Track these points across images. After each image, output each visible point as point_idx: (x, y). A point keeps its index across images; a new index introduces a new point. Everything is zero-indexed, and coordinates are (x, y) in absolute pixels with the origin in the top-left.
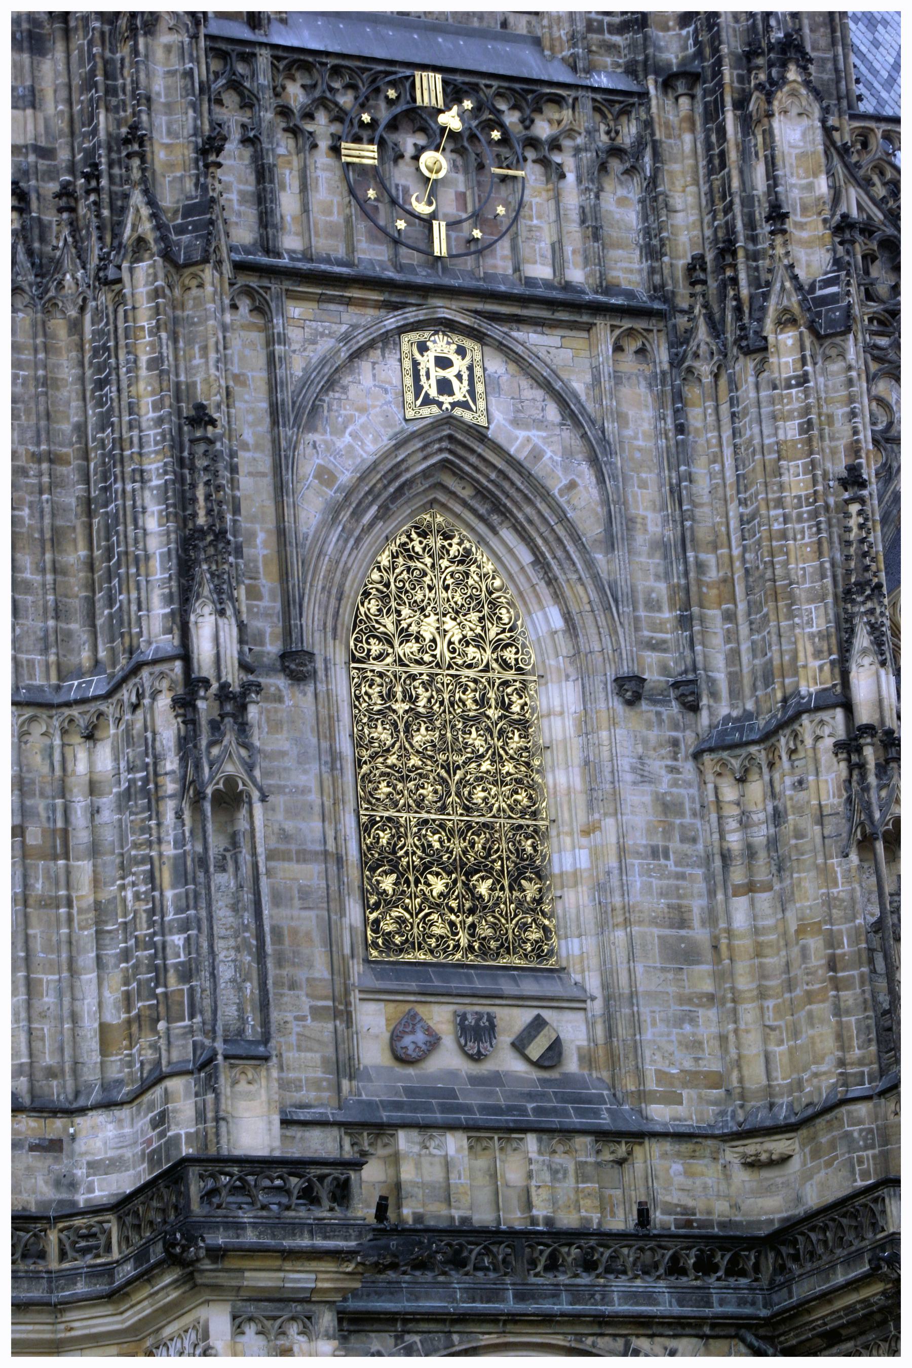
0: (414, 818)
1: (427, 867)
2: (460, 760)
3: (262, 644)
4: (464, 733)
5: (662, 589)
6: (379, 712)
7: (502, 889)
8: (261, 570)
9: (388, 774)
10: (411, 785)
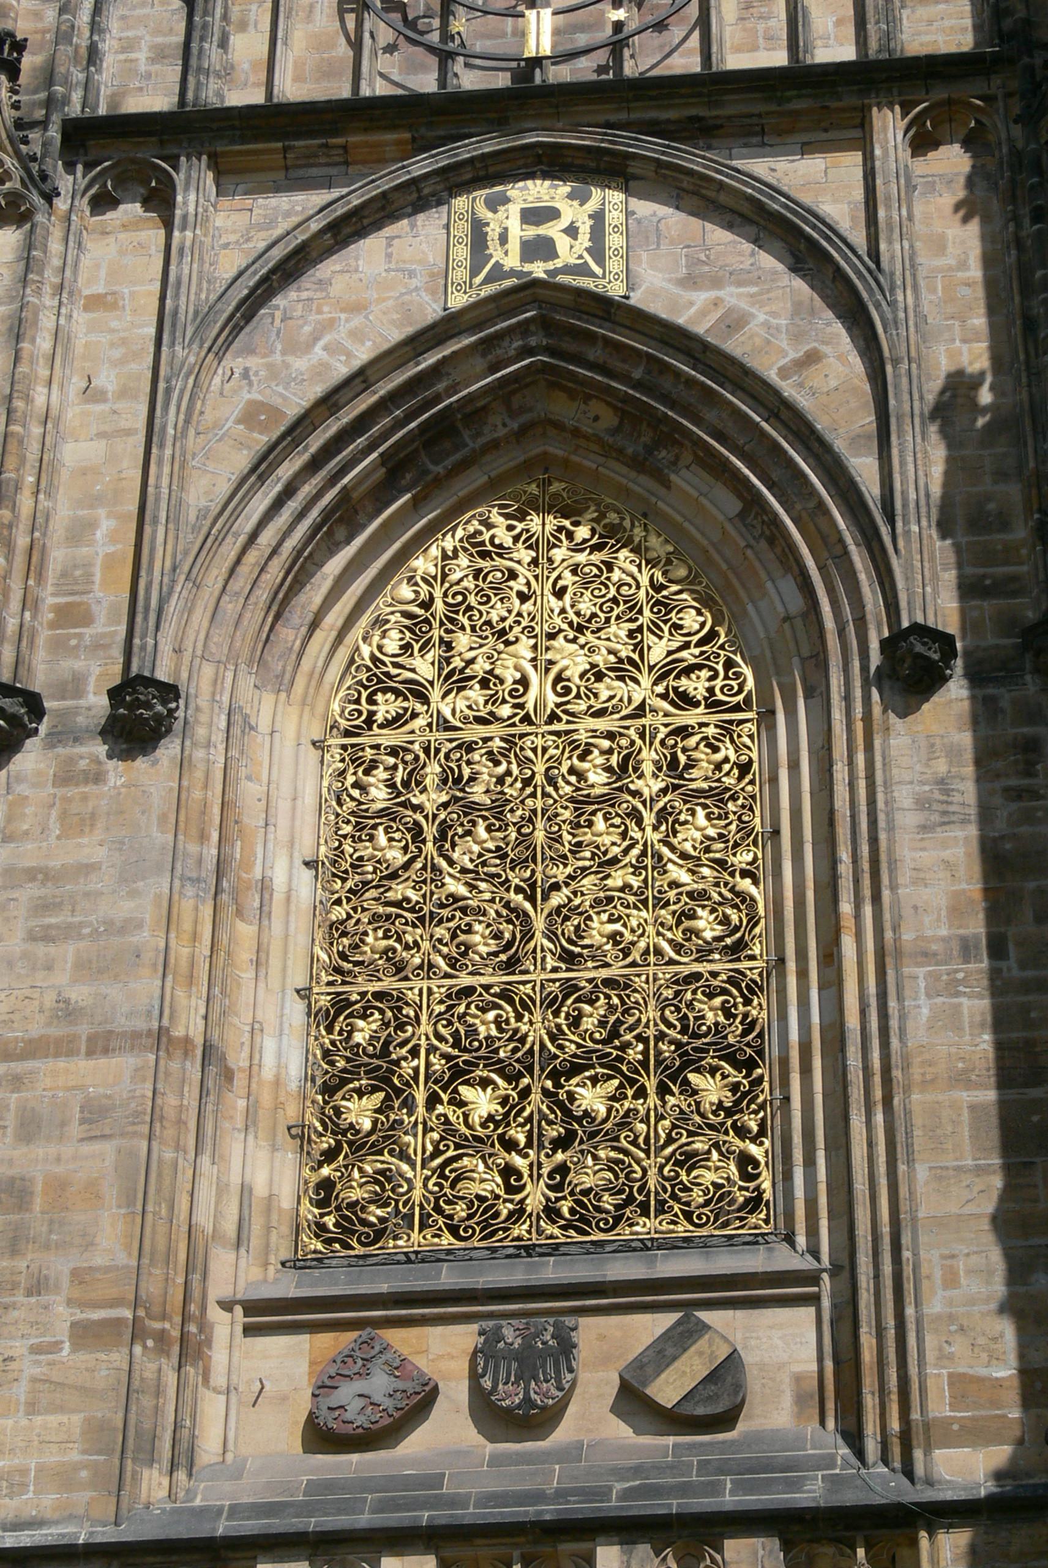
0: (440, 987)
1: (458, 1073)
2: (560, 873)
3: (79, 693)
4: (578, 826)
5: (1013, 491)
6: (382, 813)
7: (641, 1093)
8: (97, 578)
9: (388, 917)
10: (440, 932)
